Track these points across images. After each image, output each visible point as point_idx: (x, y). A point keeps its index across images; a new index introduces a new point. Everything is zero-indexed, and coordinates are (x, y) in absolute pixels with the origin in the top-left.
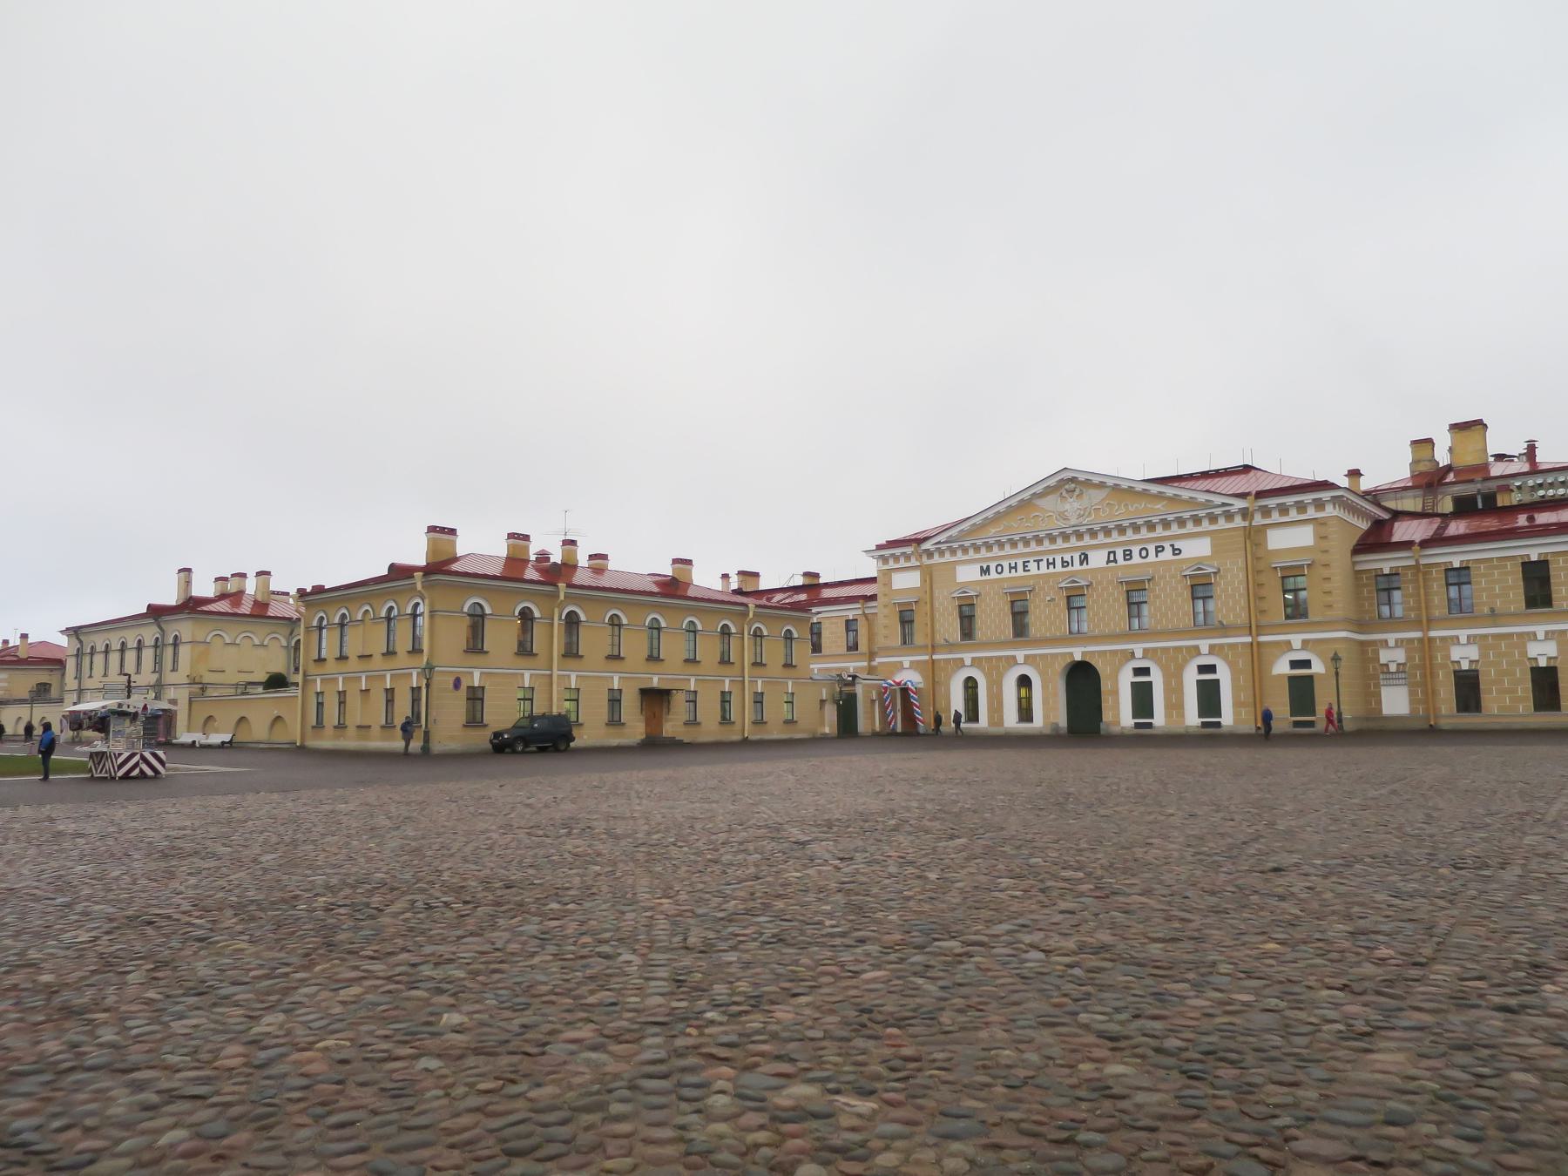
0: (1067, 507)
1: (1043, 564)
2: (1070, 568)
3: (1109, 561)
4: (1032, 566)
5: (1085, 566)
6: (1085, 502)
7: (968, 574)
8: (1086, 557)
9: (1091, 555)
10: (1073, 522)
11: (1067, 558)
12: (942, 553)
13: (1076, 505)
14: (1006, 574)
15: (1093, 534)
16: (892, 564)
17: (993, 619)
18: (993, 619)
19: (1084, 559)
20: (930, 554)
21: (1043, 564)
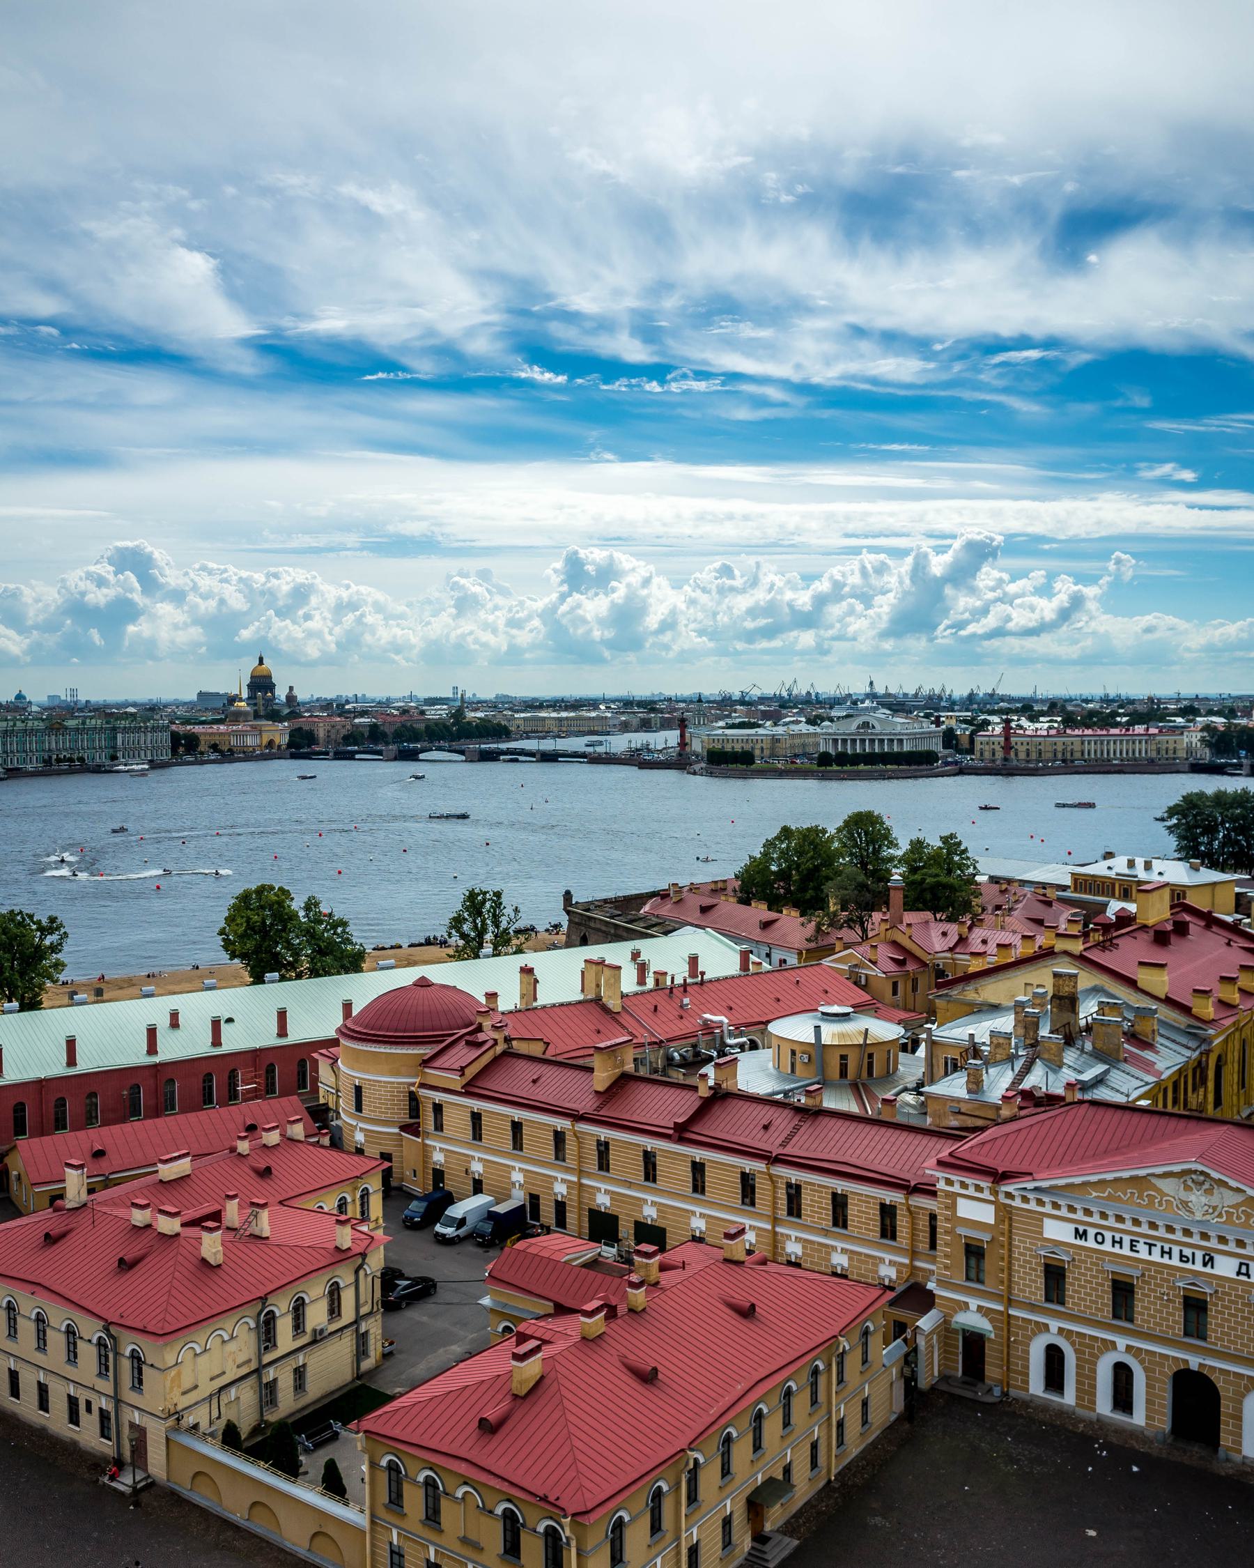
0: (1193, 1198)
1: (1156, 1251)
2: (1189, 1266)
3: (1239, 1273)
4: (1142, 1247)
5: (1208, 1270)
6: (1215, 1200)
7: (1057, 1231)
8: (1211, 1259)
9: (1217, 1258)
10: (1198, 1216)
11: (1188, 1252)
12: (1025, 1199)
13: (1204, 1200)
14: (1107, 1247)
15: (1222, 1240)
16: (956, 1188)
17: (1088, 1291)
18: (1088, 1291)
19: (1209, 1261)
20: (1009, 1195)
21: (1156, 1251)
